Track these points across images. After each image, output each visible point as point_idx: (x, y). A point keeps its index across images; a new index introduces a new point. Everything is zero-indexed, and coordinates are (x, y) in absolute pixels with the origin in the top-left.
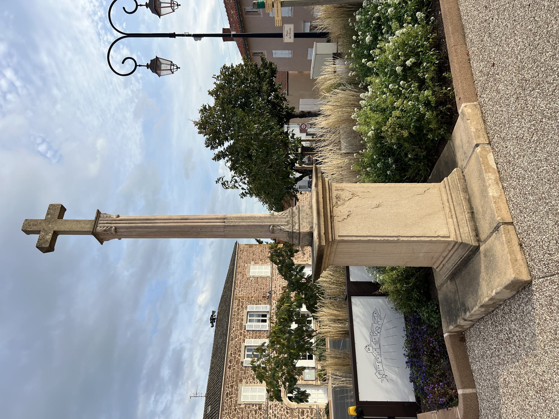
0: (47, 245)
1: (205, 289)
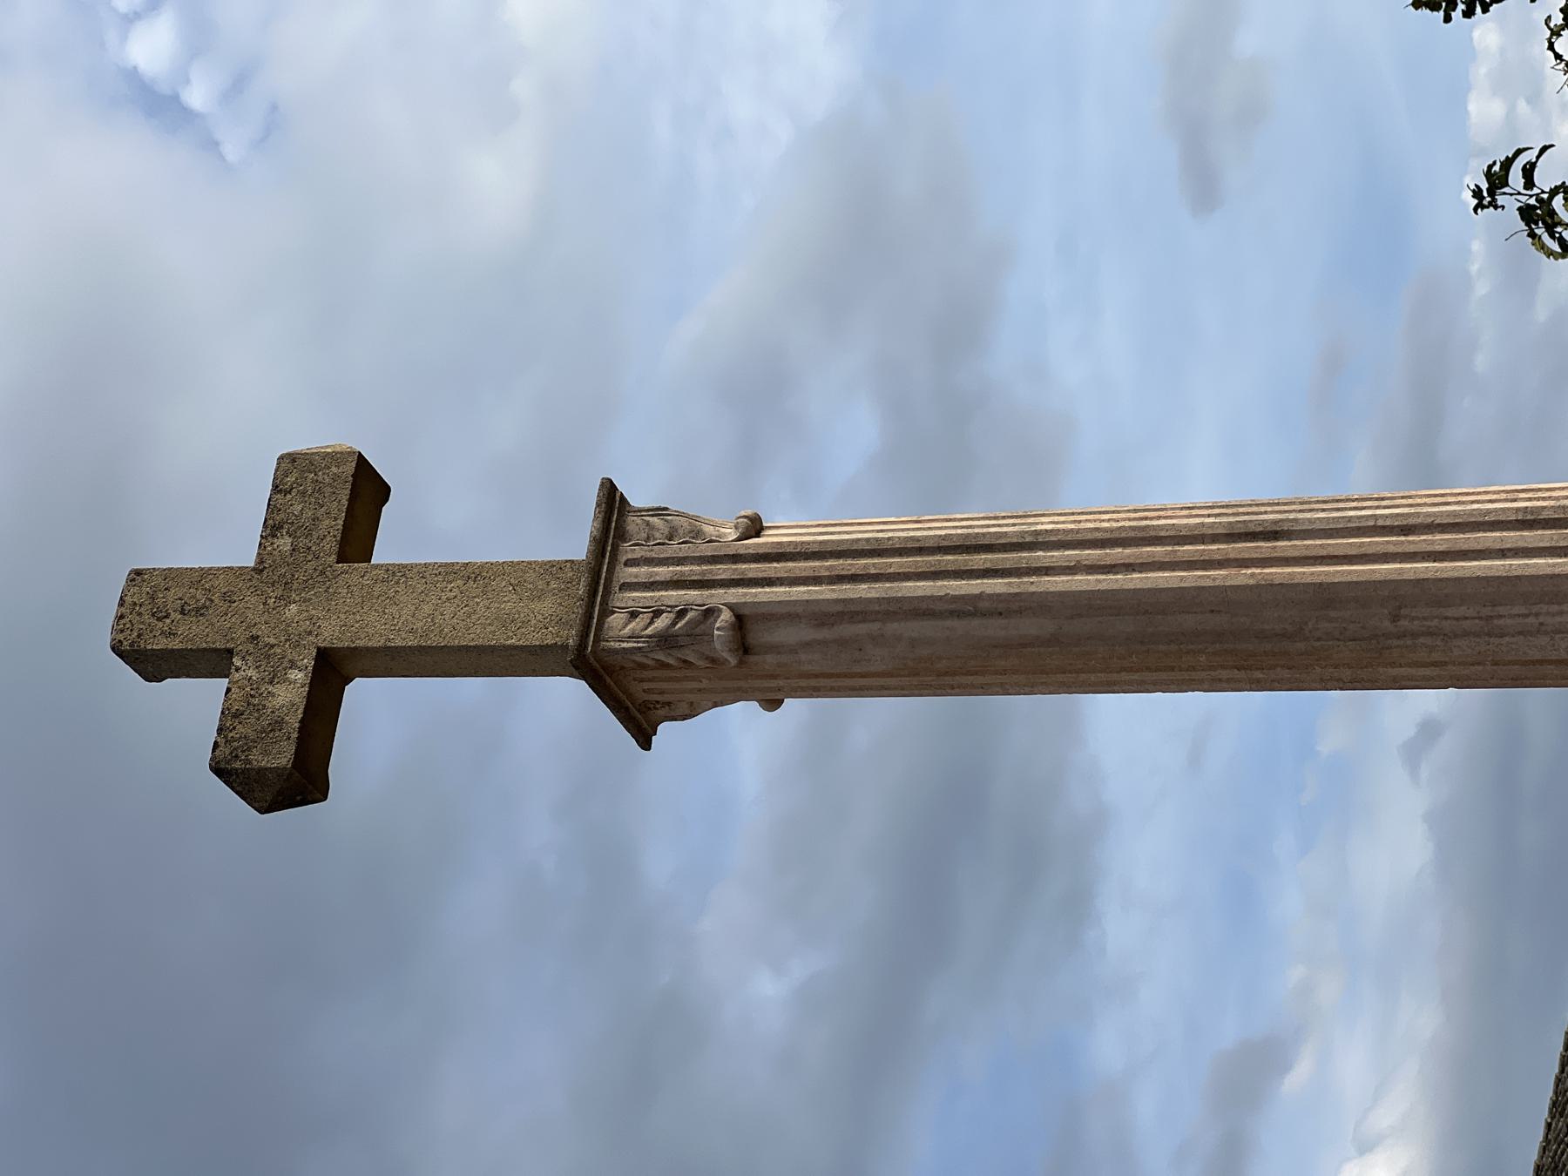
0: (282, 756)
1: (1385, 1117)
